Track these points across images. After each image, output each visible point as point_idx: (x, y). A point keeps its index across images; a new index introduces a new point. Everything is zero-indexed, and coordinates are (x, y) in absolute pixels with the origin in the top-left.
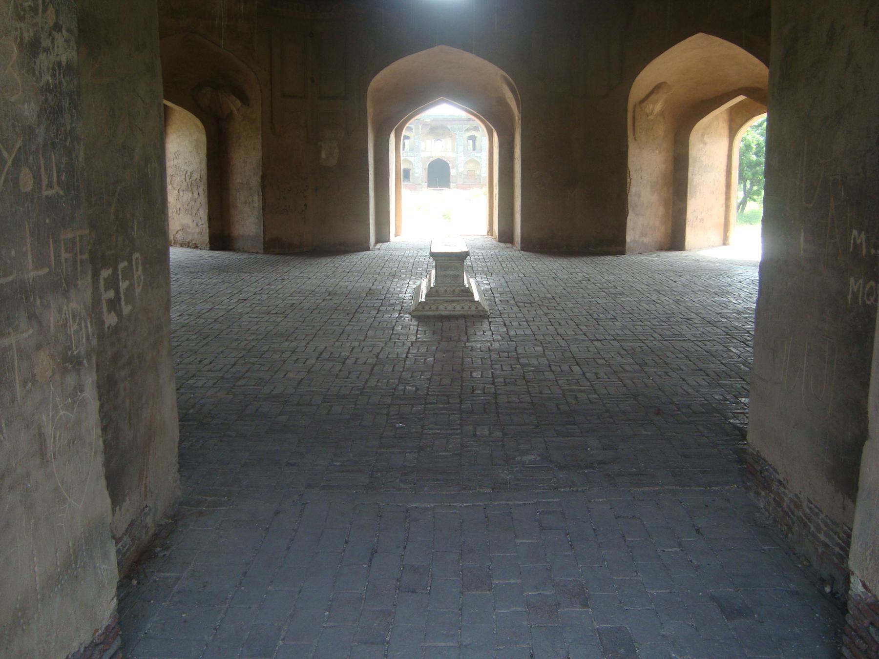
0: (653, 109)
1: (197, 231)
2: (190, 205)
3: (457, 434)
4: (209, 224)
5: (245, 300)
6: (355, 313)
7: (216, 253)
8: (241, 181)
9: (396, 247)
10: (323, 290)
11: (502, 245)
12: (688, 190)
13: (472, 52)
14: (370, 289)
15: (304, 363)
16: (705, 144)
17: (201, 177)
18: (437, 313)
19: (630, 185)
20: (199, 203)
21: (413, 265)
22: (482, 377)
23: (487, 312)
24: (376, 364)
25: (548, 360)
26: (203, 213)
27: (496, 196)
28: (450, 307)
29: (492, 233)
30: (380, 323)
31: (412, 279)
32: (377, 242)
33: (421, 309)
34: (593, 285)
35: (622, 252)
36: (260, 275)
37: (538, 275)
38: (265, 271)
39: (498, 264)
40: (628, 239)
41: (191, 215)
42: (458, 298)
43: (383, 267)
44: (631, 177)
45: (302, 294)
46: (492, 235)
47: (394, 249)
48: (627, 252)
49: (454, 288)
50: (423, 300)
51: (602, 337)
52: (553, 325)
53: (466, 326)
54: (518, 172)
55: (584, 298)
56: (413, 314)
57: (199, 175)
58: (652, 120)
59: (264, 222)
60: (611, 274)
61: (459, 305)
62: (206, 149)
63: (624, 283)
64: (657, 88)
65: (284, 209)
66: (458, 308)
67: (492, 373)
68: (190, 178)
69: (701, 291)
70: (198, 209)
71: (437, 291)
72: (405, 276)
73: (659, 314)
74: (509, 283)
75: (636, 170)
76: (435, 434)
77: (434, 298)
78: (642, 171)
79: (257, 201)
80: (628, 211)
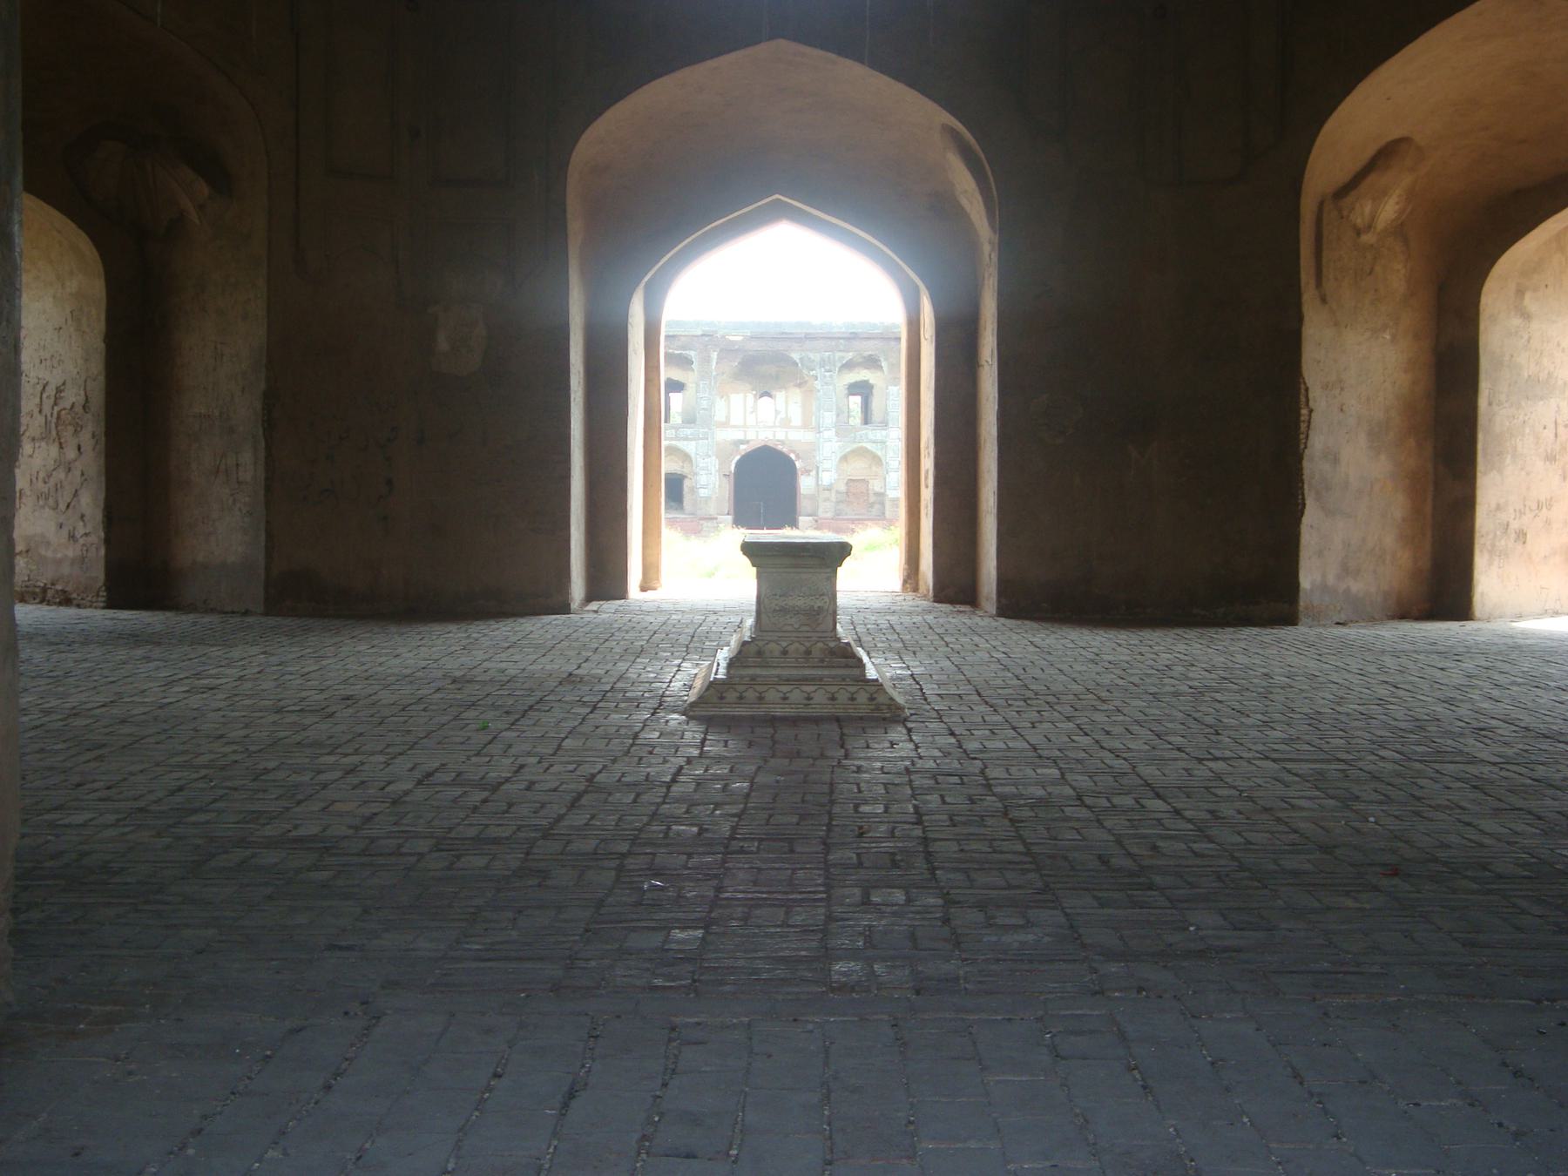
0: (1373, 217)
1: (70, 553)
2: (52, 481)
3: (821, 900)
4: (106, 534)
9: (643, 608)
10: (440, 674)
12: (1480, 446)
13: (862, 62)
15: (383, 789)
17: (87, 400)
18: (760, 711)
19: (1308, 427)
20: (79, 473)
22: (886, 812)
23: (901, 708)
24: (586, 792)
26: (90, 503)
27: (926, 478)
28: (796, 695)
29: (917, 584)
32: (590, 598)
35: (1290, 619)
40: (1307, 579)
41: (55, 508)
42: (819, 672)
44: (1311, 403)
46: (915, 590)
48: (1303, 619)
51: (1228, 754)
53: (843, 735)
54: (991, 398)
55: (1176, 694)
56: (691, 713)
57: (82, 393)
58: (1372, 245)
59: (267, 522)
61: (822, 691)
62: (103, 317)
64: (1386, 155)
66: (820, 697)
67: (915, 807)
68: (56, 404)
69: (1519, 685)
70: (76, 491)
71: (760, 653)
73: (1396, 720)
75: (1326, 387)
76: (752, 899)
77: (751, 671)
78: (1342, 389)
79: (249, 465)
80: (1303, 499)
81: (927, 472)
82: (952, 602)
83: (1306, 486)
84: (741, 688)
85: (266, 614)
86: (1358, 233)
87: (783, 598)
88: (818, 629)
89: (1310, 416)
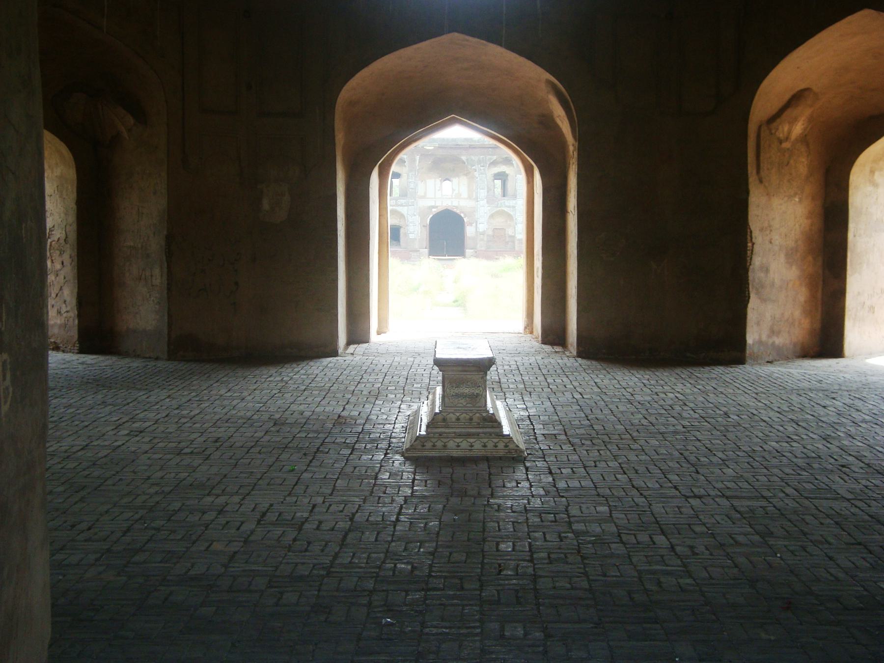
0: (790, 132)
1: (59, 322)
3: (477, 635)
5: (141, 432)
6: (316, 453)
7: (89, 359)
8: (132, 244)
10: (265, 417)
11: (548, 348)
12: (848, 260)
13: (501, 45)
14: (339, 416)
15: (238, 529)
16: (875, 185)
17: (66, 237)
18: (445, 453)
19: (752, 253)
20: (63, 277)
21: (407, 379)
22: (513, 550)
23: (522, 452)
24: (350, 530)
25: (617, 526)
27: (537, 272)
30: (355, 468)
31: (406, 401)
32: (349, 343)
33: (420, 447)
34: (692, 412)
36: (164, 394)
37: (604, 397)
38: (171, 387)
39: (541, 378)
40: (751, 338)
43: (359, 382)
44: (754, 240)
45: (232, 423)
46: (532, 333)
47: (376, 354)
48: (749, 361)
49: (471, 415)
50: (423, 433)
51: (702, 492)
52: (625, 474)
53: (490, 474)
55: (676, 433)
56: (406, 455)
57: (64, 232)
58: (788, 149)
60: (721, 395)
62: (75, 190)
63: (741, 408)
64: (797, 98)
67: (530, 544)
69: (866, 422)
70: (61, 287)
71: (444, 420)
72: (394, 396)
73: (796, 457)
74: (559, 408)
75: (762, 230)
76: (440, 634)
78: (771, 231)
79: (158, 277)
80: (749, 294)
81: (538, 268)
82: (552, 344)
84: (434, 440)
85: (169, 359)
86: (781, 142)
88: (477, 406)
89: (753, 247)
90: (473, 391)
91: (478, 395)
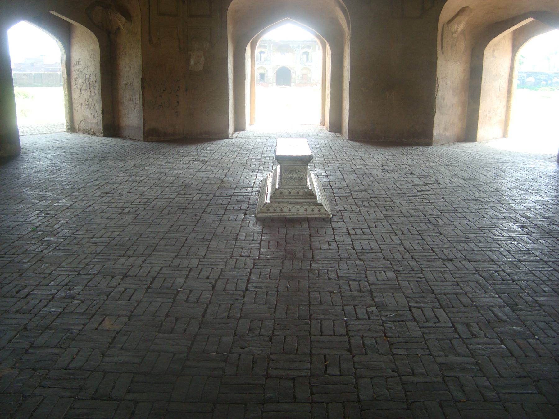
0: (457, 29)
1: (94, 121)
2: (89, 101)
4: (102, 117)
5: (107, 194)
6: (203, 213)
8: (126, 83)
11: (333, 134)
14: (222, 181)
16: (495, 57)
18: (282, 215)
21: (262, 154)
25: (406, 297)
26: (98, 108)
27: (328, 96)
30: (224, 228)
31: (261, 170)
33: (266, 211)
34: (418, 179)
35: (430, 144)
36: (132, 163)
37: (368, 167)
38: (138, 159)
39: (332, 154)
40: (435, 133)
41: (90, 109)
43: (237, 156)
45: (161, 186)
46: (324, 125)
47: (248, 137)
48: (434, 144)
50: (268, 201)
52: (396, 235)
54: (347, 77)
55: (415, 196)
56: (258, 216)
58: (456, 37)
59: (143, 115)
60: (429, 167)
61: (302, 207)
62: (99, 56)
63: (443, 177)
64: (462, 11)
65: (160, 106)
68: (89, 80)
71: (281, 193)
72: (254, 166)
74: (345, 175)
78: (446, 78)
79: (138, 99)
80: (435, 110)
81: (328, 94)
83: (436, 107)
84: (275, 206)
85: (144, 141)
87: (289, 174)
90: (299, 176)
91: (302, 178)
